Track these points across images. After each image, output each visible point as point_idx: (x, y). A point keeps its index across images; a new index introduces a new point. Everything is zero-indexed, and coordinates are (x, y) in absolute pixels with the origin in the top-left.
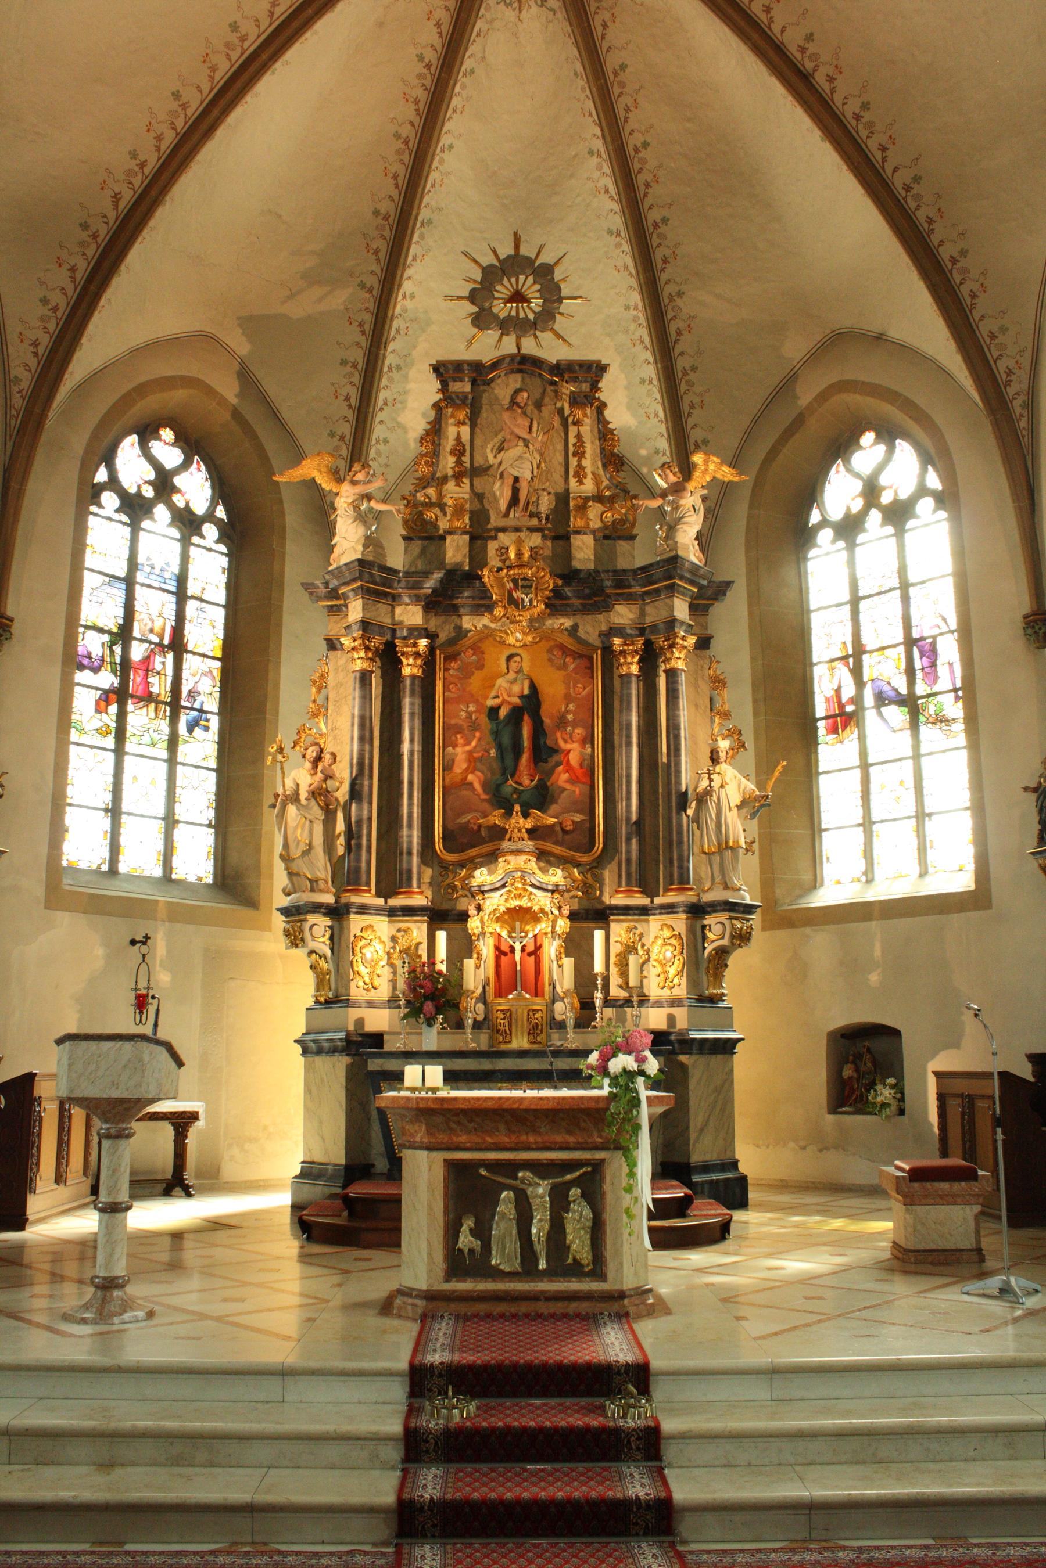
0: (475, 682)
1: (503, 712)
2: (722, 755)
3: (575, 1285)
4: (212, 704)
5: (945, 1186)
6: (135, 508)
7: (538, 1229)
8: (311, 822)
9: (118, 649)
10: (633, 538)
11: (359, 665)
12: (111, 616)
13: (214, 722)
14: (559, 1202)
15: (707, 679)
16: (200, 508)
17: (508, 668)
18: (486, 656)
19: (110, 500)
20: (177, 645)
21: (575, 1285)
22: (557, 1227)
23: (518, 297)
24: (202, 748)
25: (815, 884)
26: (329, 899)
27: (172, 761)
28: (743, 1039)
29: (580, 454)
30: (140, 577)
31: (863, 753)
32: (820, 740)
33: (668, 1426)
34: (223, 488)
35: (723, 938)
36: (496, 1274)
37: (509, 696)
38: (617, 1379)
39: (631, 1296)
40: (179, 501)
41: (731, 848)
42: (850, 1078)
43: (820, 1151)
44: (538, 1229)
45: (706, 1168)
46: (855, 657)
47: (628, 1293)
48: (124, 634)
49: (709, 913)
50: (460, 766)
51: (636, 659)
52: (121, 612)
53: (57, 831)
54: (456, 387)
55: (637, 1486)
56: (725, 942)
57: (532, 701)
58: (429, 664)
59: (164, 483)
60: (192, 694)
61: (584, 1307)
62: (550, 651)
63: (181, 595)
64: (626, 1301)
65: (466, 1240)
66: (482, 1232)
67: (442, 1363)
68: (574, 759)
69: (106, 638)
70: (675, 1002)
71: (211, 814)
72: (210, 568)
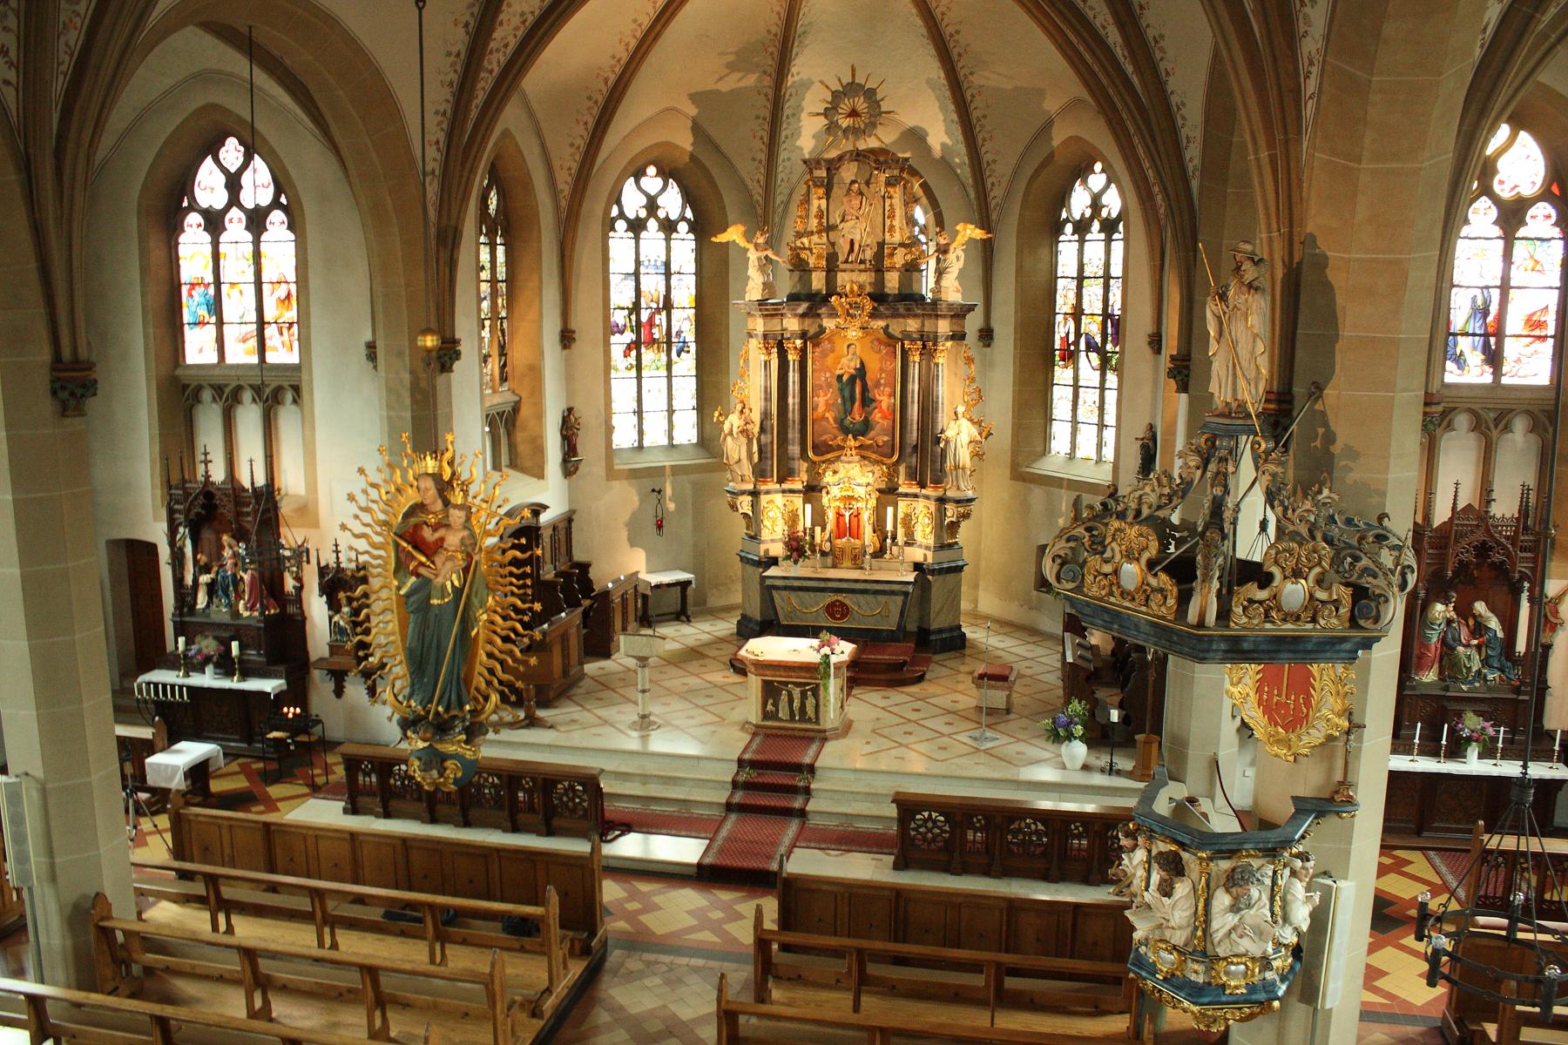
0: (830, 360)
1: (845, 378)
3: (809, 726)
4: (690, 336)
6: (636, 226)
7: (796, 704)
9: (633, 317)
11: (763, 358)
12: (628, 301)
13: (693, 347)
14: (804, 695)
16: (674, 216)
19: (621, 225)
20: (668, 305)
21: (809, 726)
22: (803, 706)
23: (853, 113)
24: (686, 364)
26: (750, 487)
27: (669, 377)
29: (892, 216)
30: (642, 270)
31: (1076, 378)
34: (689, 198)
36: (781, 720)
40: (661, 214)
44: (796, 704)
45: (940, 631)
46: (1077, 313)
48: (636, 308)
50: (821, 408)
52: (633, 294)
53: (609, 429)
54: (817, 173)
55: (797, 804)
57: (862, 371)
58: (803, 351)
59: (652, 206)
60: (679, 333)
61: (811, 734)
63: (668, 274)
65: (770, 707)
66: (776, 705)
68: (884, 406)
69: (626, 312)
70: (927, 548)
71: (694, 402)
72: (684, 249)
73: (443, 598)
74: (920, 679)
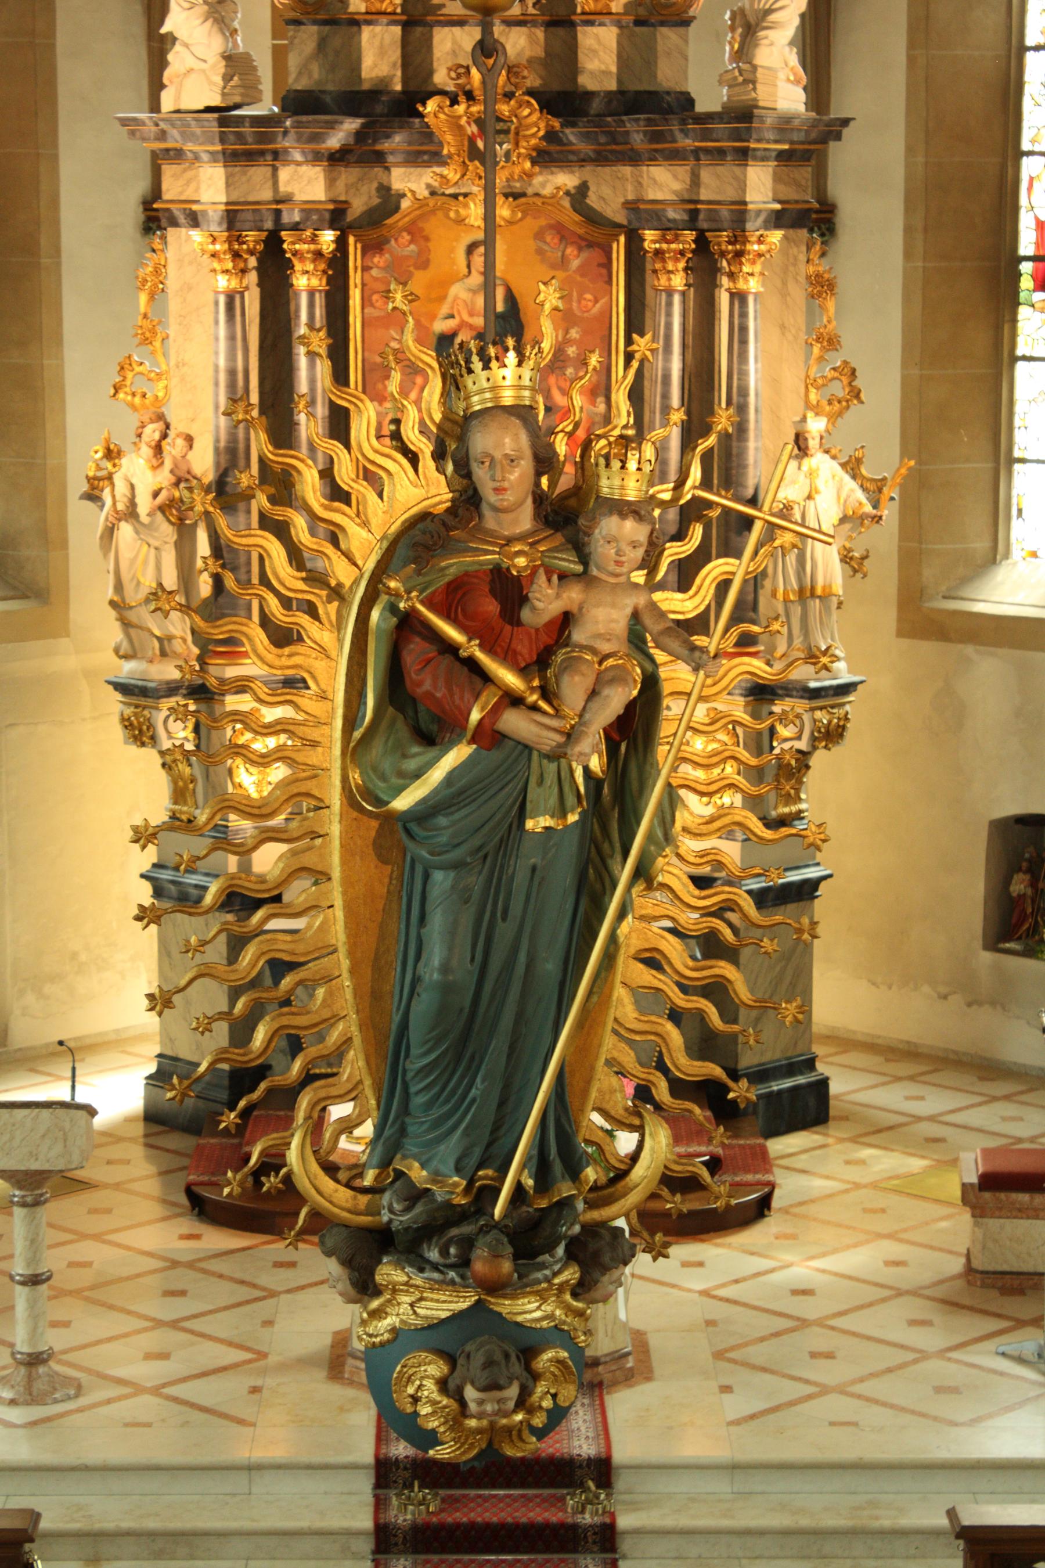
2: (813, 443)
5: (1024, 1198)
8: (156, 549)
10: (686, 23)
11: (223, 282)
15: (802, 279)
17: (469, 266)
18: (431, 245)
25: (995, 553)
28: (830, 876)
32: (1023, 296)
33: (624, 1522)
35: (799, 738)
37: (471, 315)
38: (579, 1472)
39: (606, 1363)
41: (819, 597)
42: (1022, 897)
43: (969, 1005)
47: (603, 1360)
49: (781, 697)
51: (681, 265)
56: (803, 745)
58: (336, 267)
62: (539, 236)
64: (601, 1368)
67: (407, 1457)
73: (562, 812)
74: (762, 1207)
